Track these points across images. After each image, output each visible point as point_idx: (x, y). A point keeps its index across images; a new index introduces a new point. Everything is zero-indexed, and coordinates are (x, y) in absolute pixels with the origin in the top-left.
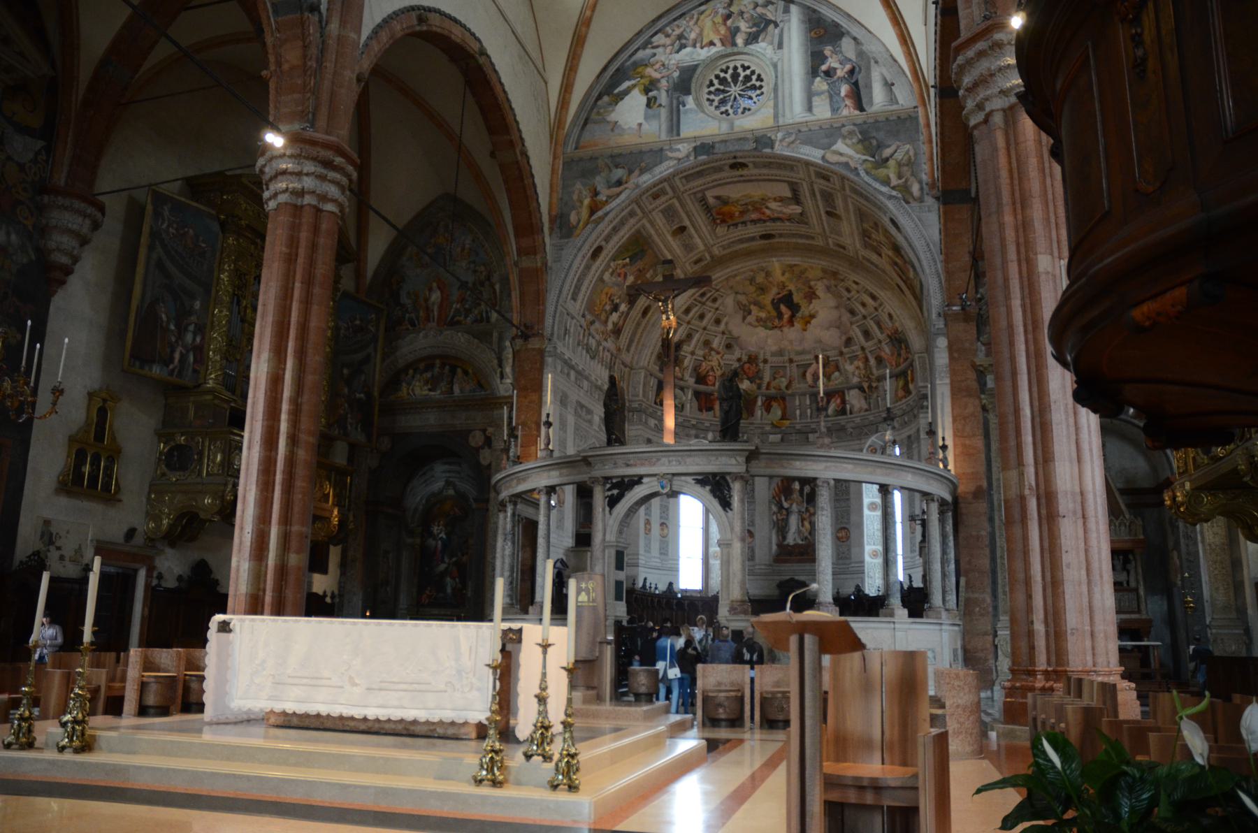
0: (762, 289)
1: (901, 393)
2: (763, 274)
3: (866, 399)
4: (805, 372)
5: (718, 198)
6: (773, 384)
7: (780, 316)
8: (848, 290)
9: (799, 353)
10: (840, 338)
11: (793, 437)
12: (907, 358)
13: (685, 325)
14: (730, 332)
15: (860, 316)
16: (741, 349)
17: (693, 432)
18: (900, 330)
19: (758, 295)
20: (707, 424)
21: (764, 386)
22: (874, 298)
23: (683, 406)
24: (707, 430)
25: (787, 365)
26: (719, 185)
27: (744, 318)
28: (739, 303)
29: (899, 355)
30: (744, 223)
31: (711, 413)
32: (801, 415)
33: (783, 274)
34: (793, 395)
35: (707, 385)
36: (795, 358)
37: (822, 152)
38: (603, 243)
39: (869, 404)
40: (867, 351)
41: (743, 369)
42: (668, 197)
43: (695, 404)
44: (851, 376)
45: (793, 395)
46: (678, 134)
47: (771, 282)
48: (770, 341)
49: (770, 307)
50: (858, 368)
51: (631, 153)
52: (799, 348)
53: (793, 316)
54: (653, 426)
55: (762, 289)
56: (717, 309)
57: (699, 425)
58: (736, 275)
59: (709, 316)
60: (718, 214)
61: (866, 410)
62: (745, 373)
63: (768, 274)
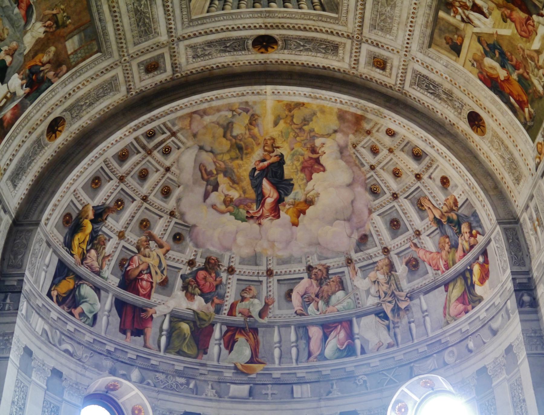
0: (240, 149)
1: (455, 308)
2: (245, 119)
3: (388, 327)
4: (291, 291)
6: (240, 307)
7: (261, 198)
8: (375, 151)
9: (283, 262)
10: (350, 237)
11: (270, 390)
12: (472, 247)
14: (182, 215)
15: (388, 195)
16: (197, 245)
17: (108, 363)
18: (460, 203)
19: (232, 159)
20: (132, 355)
21: (226, 308)
22: (418, 156)
23: (95, 317)
24: (130, 364)
25: (264, 279)
27: (206, 196)
28: (201, 168)
29: (454, 246)
31: (140, 339)
32: (280, 358)
33: (276, 124)
34: (270, 326)
35: (137, 293)
36: (276, 269)
39: (395, 335)
40: (392, 254)
41: (195, 278)
43: (116, 320)
44: (363, 295)
45: (270, 326)
47: (254, 137)
48: (240, 240)
49: (246, 183)
50: (376, 282)
52: (284, 254)
53: (279, 201)
54: (39, 330)
55: (240, 149)
56: (168, 169)
57: (118, 354)
59: (153, 178)
61: (389, 346)
62: (198, 285)
63: (253, 120)
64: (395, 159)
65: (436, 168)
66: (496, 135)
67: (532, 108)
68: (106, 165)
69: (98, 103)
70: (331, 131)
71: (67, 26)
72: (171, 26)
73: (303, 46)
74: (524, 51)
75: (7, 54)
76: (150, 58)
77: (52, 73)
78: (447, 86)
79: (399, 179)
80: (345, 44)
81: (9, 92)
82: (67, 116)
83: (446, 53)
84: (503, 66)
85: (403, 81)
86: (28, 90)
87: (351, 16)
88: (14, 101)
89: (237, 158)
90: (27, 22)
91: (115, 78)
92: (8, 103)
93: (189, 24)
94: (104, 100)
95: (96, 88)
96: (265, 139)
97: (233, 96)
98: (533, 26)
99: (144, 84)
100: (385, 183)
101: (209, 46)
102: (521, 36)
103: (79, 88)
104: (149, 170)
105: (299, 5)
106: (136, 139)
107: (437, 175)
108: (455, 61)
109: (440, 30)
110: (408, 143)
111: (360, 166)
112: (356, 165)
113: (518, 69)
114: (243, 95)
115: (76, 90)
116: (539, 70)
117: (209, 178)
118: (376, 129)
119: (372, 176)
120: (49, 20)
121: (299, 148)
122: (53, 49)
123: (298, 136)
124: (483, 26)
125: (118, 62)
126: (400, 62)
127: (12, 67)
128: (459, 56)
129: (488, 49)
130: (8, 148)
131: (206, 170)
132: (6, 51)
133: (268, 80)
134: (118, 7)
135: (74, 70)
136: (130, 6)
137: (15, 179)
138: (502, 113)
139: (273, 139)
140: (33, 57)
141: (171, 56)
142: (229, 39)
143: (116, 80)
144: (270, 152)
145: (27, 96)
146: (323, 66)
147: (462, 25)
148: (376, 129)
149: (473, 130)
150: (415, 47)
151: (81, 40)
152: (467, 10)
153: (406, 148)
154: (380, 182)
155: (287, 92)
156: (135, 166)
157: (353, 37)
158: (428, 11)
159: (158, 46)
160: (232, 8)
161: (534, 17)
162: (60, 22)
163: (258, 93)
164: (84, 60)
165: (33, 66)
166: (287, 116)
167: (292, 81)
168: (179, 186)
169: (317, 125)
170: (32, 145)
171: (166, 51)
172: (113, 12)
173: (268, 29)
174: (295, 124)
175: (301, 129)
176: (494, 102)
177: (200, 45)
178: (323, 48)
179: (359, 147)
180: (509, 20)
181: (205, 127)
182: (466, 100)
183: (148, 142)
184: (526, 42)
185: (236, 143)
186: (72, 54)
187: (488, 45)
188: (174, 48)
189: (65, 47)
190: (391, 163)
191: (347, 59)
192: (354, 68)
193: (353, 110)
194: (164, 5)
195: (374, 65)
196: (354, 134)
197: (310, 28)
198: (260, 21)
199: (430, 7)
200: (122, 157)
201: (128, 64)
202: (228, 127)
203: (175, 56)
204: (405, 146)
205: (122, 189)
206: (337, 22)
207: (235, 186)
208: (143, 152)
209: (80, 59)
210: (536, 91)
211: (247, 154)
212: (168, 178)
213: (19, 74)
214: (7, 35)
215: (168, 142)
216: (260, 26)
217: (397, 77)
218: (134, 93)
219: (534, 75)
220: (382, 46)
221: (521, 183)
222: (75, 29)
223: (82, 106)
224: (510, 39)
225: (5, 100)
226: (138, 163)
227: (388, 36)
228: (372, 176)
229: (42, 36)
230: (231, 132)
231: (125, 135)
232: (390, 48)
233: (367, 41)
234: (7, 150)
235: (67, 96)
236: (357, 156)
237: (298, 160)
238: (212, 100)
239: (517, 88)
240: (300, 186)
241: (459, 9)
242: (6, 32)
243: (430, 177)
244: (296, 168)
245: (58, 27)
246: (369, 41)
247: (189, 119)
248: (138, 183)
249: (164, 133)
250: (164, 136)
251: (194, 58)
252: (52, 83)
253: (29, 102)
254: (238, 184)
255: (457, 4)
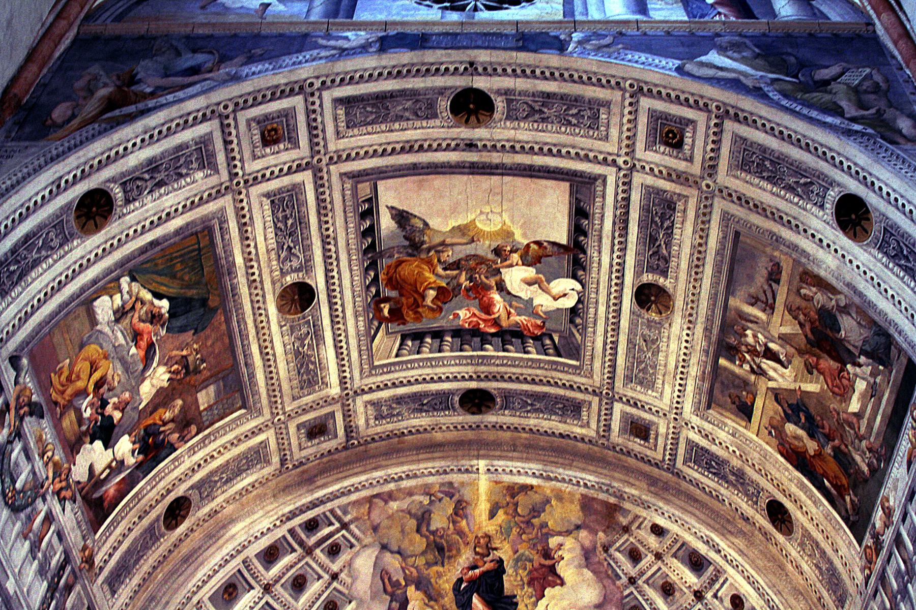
0: (441, 549)
5: (402, 217)
8: (635, 556)
13: (257, 592)
19: (429, 565)
22: (697, 563)
26: (415, 170)
30: (438, 335)
33: (492, 515)
37: (677, 63)
38: (117, 192)
42: (293, 154)
46: (350, 13)
47: (461, 533)
49: (449, 600)
51: (235, 36)
55: (441, 549)
56: (335, 577)
58: (389, 497)
59: (314, 588)
60: (392, 283)
63: (461, 509)
64: (664, 568)
65: (724, 582)
66: (807, 534)
67: (856, 495)
68: (246, 567)
69: (239, 478)
70: (572, 527)
71: (200, 372)
72: (345, 374)
73: (532, 405)
74: (838, 414)
75: (116, 408)
76: (315, 418)
77: (176, 435)
78: (736, 463)
79: (671, 598)
80: (590, 403)
81: (115, 459)
82: (195, 496)
83: (733, 417)
84: (812, 436)
85: (674, 456)
86: (141, 457)
87: (597, 364)
88: (120, 473)
89: (436, 563)
90: (146, 367)
91: (264, 444)
92: (113, 475)
93: (370, 372)
94: (248, 475)
95: (237, 458)
96: (476, 537)
97: (431, 474)
98: (849, 380)
99: (304, 453)
100: (651, 604)
101: (399, 403)
102: (833, 393)
103: (212, 457)
104: (308, 576)
105: (524, 348)
106: (291, 531)
107: (725, 592)
108: (746, 428)
109: (722, 383)
110: (683, 545)
111: (614, 578)
112: (608, 576)
113: (834, 440)
114: (445, 472)
115: (209, 460)
116: (861, 441)
117: (394, 592)
118: (636, 524)
119: (632, 593)
120: (176, 363)
121: (523, 550)
122: (179, 402)
123: (524, 533)
124: (780, 380)
125: (270, 424)
126: (668, 428)
127: (121, 426)
128: (750, 421)
129: (790, 412)
130: (107, 538)
131: (390, 579)
132: (114, 403)
133: (482, 452)
134: (273, 348)
135: (206, 432)
136: (288, 347)
137: (114, 582)
138: (816, 502)
139: (488, 537)
140: (152, 413)
141: (344, 415)
142: (426, 394)
143: (266, 447)
144: (483, 556)
145: (139, 466)
146: (560, 434)
147: (753, 377)
148: (636, 524)
149: (776, 527)
150: (688, 407)
151: (218, 393)
152: (758, 356)
153: (681, 553)
154: (643, 603)
155: (508, 470)
156: (288, 570)
157: (601, 393)
158: (704, 358)
159: (326, 401)
160: (431, 352)
161: (849, 366)
162: (191, 368)
163: (467, 471)
164: (222, 418)
165: (150, 425)
166: (508, 504)
167: (515, 454)
168: (350, 602)
169: (554, 517)
170: (142, 534)
171: (337, 408)
172: (264, 354)
173: (482, 380)
174: (519, 515)
175: (528, 523)
176: (802, 487)
177: (385, 401)
178: (559, 408)
179: (612, 550)
180: (815, 372)
181: (390, 517)
182: (763, 482)
183: (308, 537)
184: (841, 402)
185: (434, 541)
186: (205, 409)
187: (789, 405)
188: (349, 405)
189: (197, 399)
190: (659, 574)
191: (594, 425)
192: (604, 436)
193: (602, 496)
194: (335, 346)
195: (631, 433)
196: (604, 531)
197: (541, 381)
198: (470, 369)
199: (707, 352)
200: (270, 555)
201: (283, 426)
202: (423, 518)
203: (350, 416)
204: (679, 549)
205: (267, 603)
206: (578, 372)
207: (432, 603)
208: (300, 550)
209: (216, 417)
210: (859, 471)
211: (450, 558)
212: (335, 588)
213: (130, 436)
214: (119, 382)
215: (336, 537)
216: (471, 377)
217: (665, 450)
218: (291, 466)
219: (854, 448)
220: (642, 406)
221: (846, 606)
222: (211, 377)
223: (216, 482)
224: (818, 396)
225: (108, 471)
226: (292, 567)
227: (650, 392)
228: (632, 593)
229: (166, 384)
230: (428, 525)
231: (275, 525)
232: (654, 409)
233: (621, 398)
234: (105, 542)
235: (196, 468)
236: (609, 564)
237: (525, 569)
238: (401, 478)
239: (832, 467)
240: (526, 606)
241: (746, 355)
242: (116, 378)
243: (715, 596)
244: (522, 579)
245: (187, 373)
246: (624, 399)
247: (368, 506)
248: (290, 595)
249: (331, 524)
250: (332, 528)
251: (376, 419)
252: (176, 450)
253: (141, 475)
254: (436, 601)
255: (743, 348)
